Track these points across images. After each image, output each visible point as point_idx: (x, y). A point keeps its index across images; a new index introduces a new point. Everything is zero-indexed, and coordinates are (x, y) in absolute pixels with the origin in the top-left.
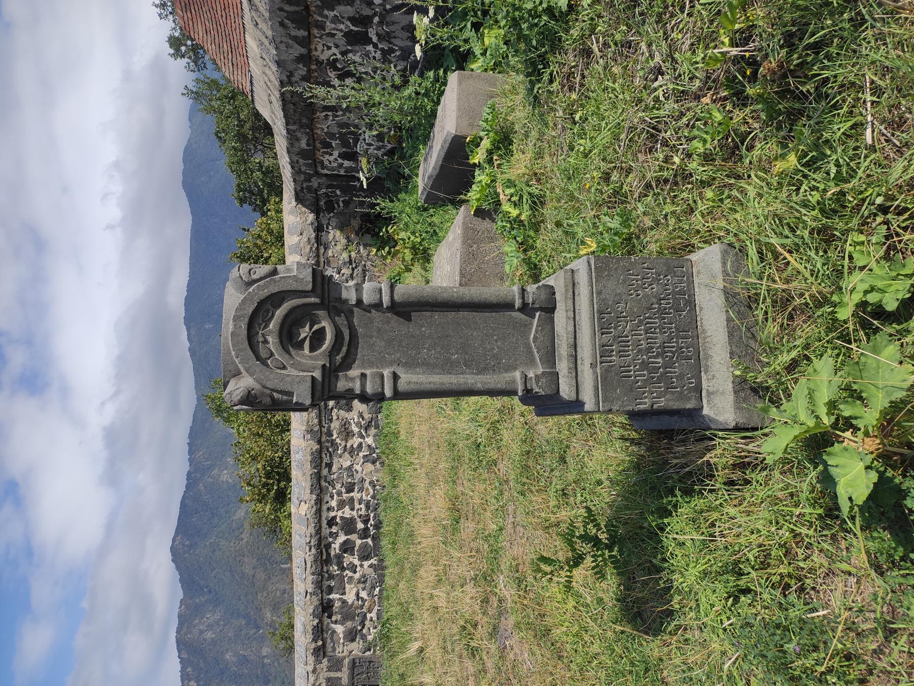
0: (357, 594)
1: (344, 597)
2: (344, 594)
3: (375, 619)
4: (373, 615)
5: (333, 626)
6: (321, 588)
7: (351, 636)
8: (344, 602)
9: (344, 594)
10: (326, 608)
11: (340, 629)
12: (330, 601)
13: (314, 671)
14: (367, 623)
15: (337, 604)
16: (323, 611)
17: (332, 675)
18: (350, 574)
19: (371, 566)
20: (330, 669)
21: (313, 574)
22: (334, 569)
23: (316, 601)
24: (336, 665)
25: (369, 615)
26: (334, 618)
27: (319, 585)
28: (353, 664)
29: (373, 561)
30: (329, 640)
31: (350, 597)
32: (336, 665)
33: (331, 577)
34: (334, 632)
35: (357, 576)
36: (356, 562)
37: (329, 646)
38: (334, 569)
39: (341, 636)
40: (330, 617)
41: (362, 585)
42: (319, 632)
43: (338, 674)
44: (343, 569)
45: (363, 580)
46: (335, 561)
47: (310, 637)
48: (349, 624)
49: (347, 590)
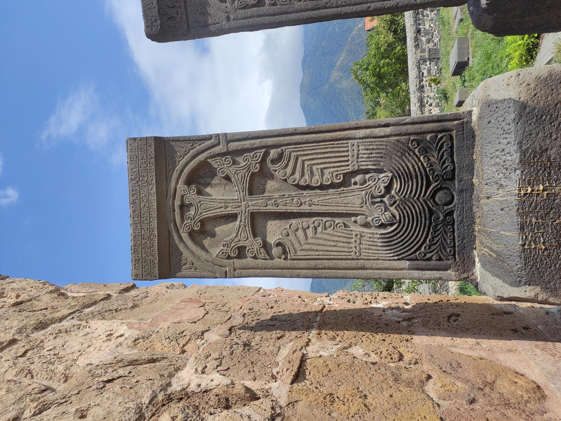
0: (430, 25)
1: (425, 27)
2: (424, 25)
3: (437, 34)
4: (436, 32)
5: (421, 38)
6: (416, 23)
7: (428, 41)
8: (425, 29)
9: (424, 25)
10: (418, 31)
11: (424, 39)
12: (419, 28)
13: (415, 53)
14: (434, 36)
15: (422, 30)
16: (418, 33)
17: (422, 54)
18: (427, 18)
19: (434, 14)
20: (421, 52)
21: (413, 18)
22: (420, 16)
23: (414, 27)
24: (423, 51)
25: (434, 33)
26: (421, 35)
27: (415, 21)
28: (430, 51)
29: (435, 12)
30: (420, 43)
31: (427, 27)
32: (423, 51)
33: (419, 20)
34: (422, 40)
35: (429, 18)
36: (429, 13)
37: (420, 47)
38: (420, 16)
39: (424, 41)
40: (420, 34)
41: (431, 22)
42: (416, 39)
43: (424, 54)
44: (424, 16)
45: (432, 20)
46: (421, 13)
47: (413, 41)
48: (427, 36)
49: (426, 24)
